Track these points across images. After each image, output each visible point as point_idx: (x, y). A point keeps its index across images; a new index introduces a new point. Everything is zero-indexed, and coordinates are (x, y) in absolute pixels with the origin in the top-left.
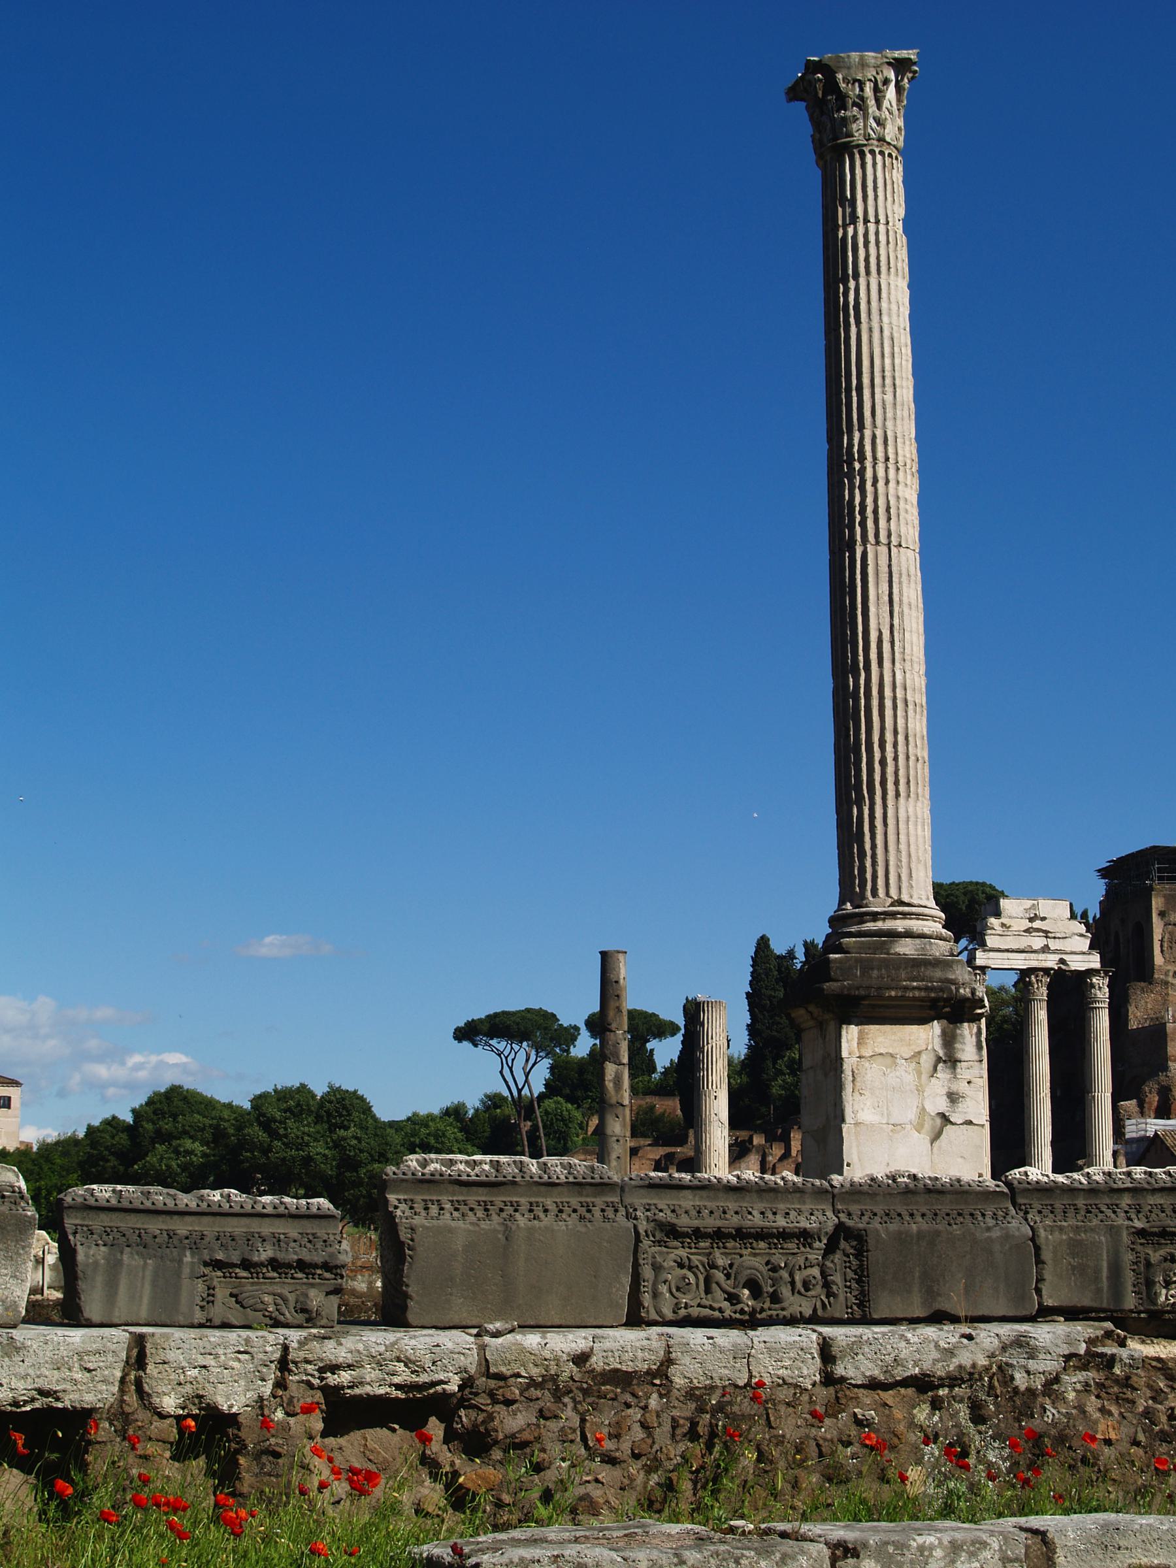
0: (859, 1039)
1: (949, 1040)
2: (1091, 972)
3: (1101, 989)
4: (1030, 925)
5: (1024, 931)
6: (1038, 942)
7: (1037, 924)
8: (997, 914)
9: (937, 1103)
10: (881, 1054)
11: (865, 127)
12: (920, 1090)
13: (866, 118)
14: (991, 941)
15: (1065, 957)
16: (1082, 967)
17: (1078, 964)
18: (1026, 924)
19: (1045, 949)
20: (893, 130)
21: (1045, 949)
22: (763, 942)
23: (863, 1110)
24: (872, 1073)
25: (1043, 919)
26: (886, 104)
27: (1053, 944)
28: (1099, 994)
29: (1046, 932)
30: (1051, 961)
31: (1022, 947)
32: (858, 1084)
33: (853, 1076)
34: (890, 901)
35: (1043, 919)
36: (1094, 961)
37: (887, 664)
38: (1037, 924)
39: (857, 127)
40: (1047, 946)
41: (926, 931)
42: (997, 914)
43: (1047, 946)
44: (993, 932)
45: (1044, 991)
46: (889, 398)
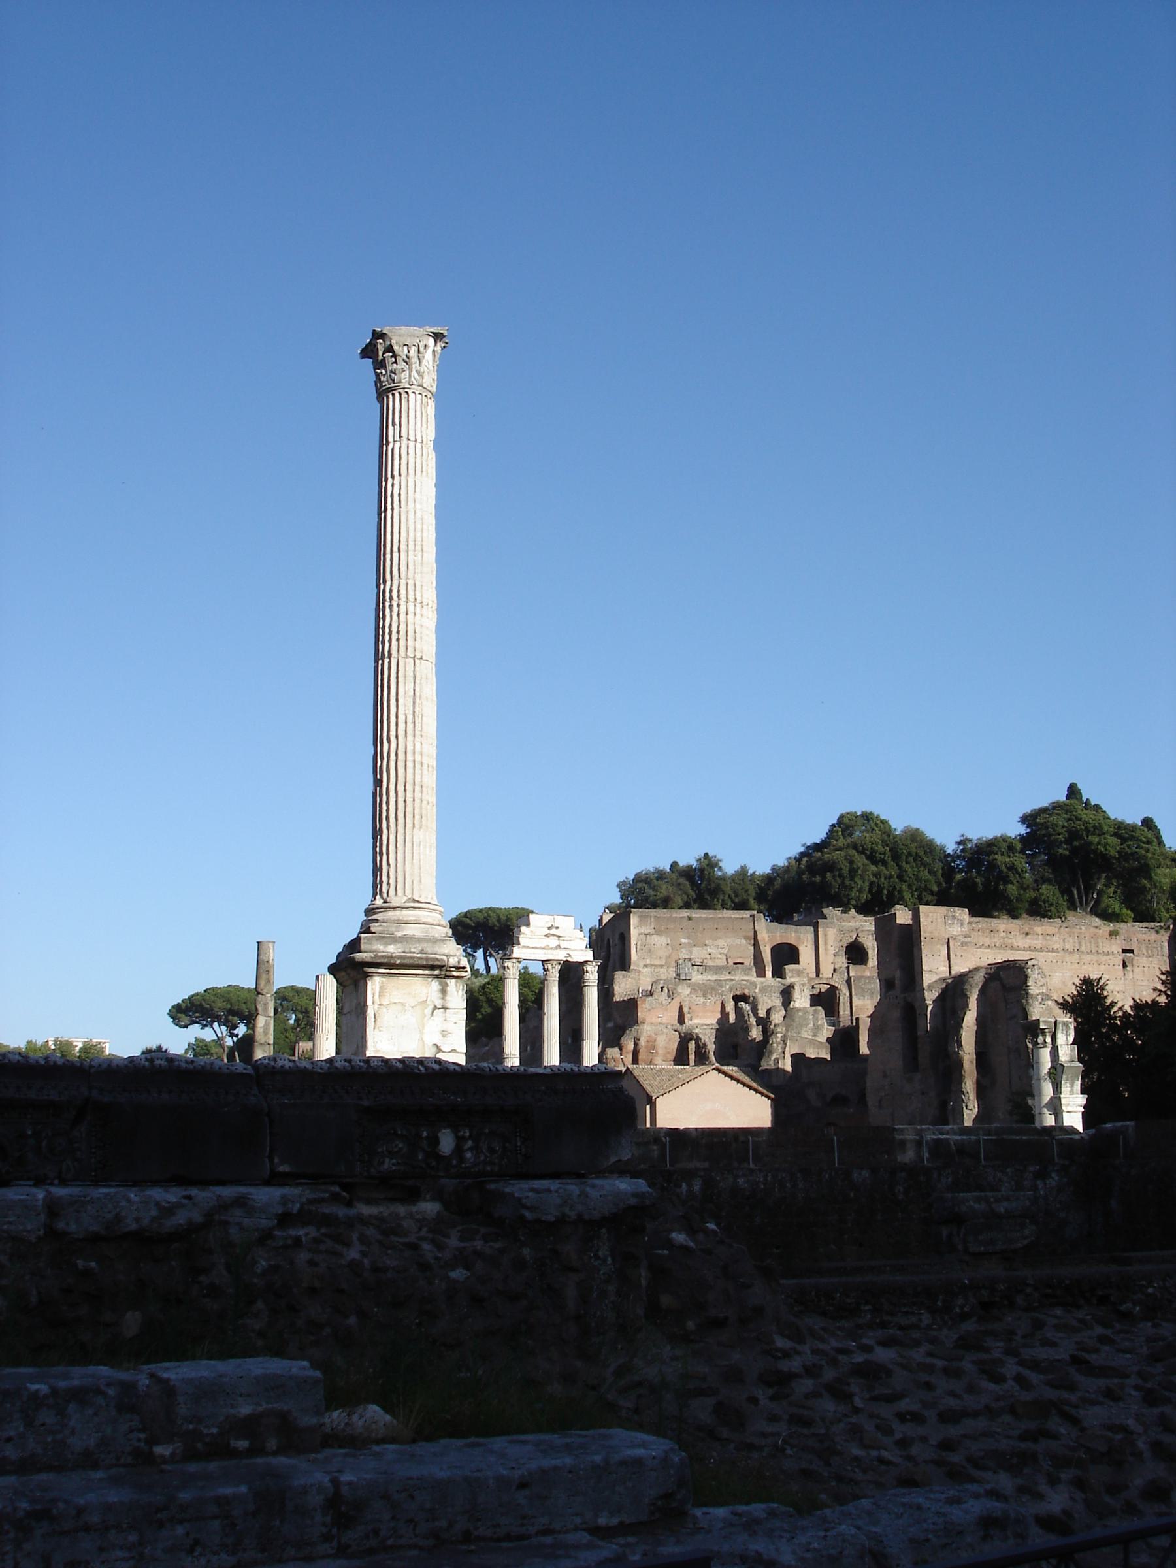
0: (380, 993)
1: (443, 991)
2: (586, 962)
3: (592, 976)
4: (548, 932)
5: (545, 936)
6: (553, 942)
7: (553, 931)
8: (528, 924)
10: (395, 1003)
11: (410, 376)
12: (422, 1027)
13: (411, 370)
15: (570, 953)
16: (582, 960)
17: (577, 957)
20: (430, 380)
23: (381, 1041)
24: (387, 1016)
25: (557, 928)
26: (424, 362)
28: (592, 977)
29: (559, 937)
30: (562, 956)
31: (543, 946)
32: (378, 1024)
33: (375, 1017)
34: (406, 898)
35: (557, 928)
36: (588, 955)
37: (410, 738)
38: (553, 931)
40: (559, 945)
41: (430, 920)
42: (528, 924)
43: (559, 945)
44: (524, 936)
46: (419, 558)
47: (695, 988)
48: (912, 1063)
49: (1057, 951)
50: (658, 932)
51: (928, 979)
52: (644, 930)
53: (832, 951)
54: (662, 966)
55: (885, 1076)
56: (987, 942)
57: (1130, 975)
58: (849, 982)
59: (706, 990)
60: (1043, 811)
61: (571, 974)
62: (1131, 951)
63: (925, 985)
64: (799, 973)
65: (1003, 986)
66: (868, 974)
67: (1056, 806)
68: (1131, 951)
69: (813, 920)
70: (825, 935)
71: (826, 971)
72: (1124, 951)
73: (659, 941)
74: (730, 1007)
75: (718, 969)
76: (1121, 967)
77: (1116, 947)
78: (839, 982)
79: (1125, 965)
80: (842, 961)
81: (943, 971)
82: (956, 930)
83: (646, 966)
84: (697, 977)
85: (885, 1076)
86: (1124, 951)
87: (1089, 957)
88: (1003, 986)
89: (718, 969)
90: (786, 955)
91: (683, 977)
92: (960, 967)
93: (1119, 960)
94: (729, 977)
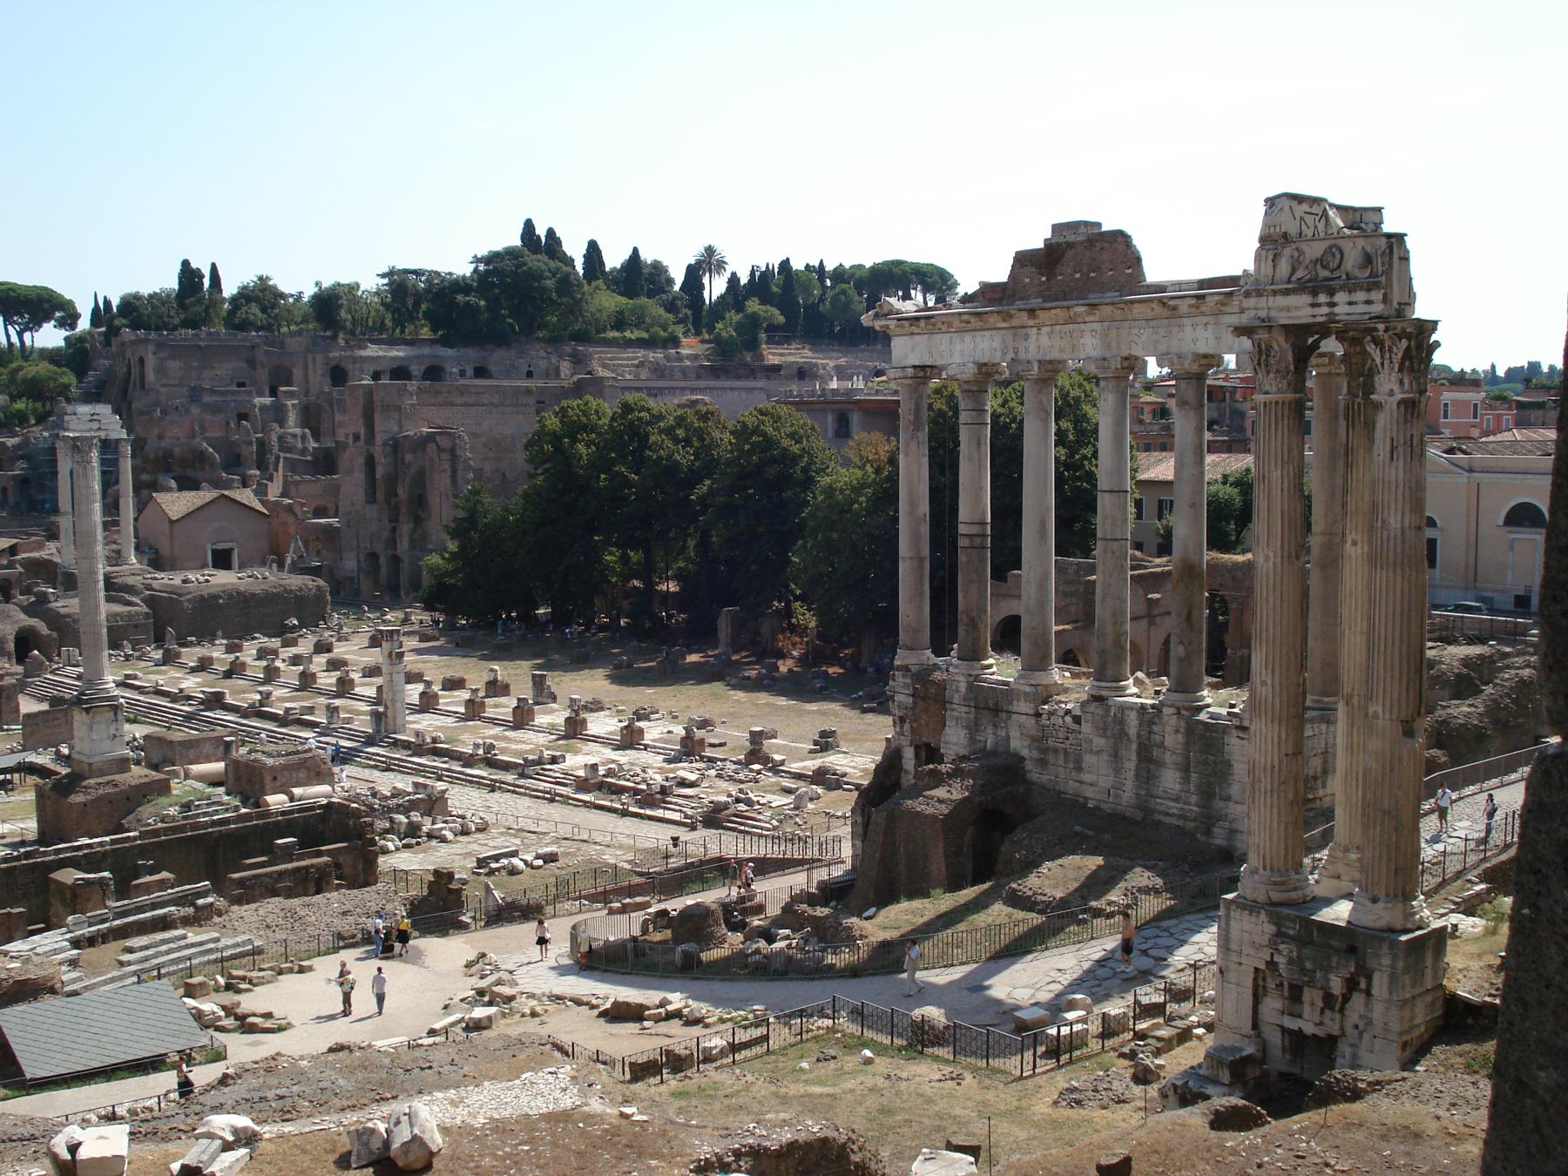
3: (128, 450)
6: (95, 425)
9: (112, 731)
17: (114, 436)
19: (99, 429)
21: (99, 429)
30: (103, 434)
48: (371, 498)
59: (215, 409)
61: (108, 446)
62: (543, 402)
64: (291, 395)
65: (438, 447)
67: (510, 253)
68: (543, 402)
70: (314, 359)
72: (538, 402)
83: (163, 385)
84: (207, 399)
86: (538, 402)
88: (438, 447)
93: (533, 410)
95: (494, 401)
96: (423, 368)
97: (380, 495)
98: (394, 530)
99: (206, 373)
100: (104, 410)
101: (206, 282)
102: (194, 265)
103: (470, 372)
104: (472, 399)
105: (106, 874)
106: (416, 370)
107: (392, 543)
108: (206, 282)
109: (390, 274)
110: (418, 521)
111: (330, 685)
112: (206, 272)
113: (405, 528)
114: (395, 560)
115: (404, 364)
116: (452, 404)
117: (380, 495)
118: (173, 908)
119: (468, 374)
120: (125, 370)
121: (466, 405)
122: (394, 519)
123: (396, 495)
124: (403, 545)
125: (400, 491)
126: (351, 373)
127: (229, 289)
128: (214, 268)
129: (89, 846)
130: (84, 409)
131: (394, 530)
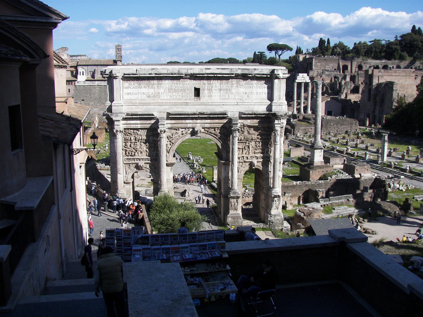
1: (321, 150)
2: (309, 82)
6: (303, 79)
7: (303, 77)
8: (298, 75)
9: (320, 155)
14: (298, 79)
16: (308, 82)
17: (307, 81)
18: (302, 77)
22: (255, 52)
24: (316, 153)
27: (305, 79)
30: (304, 81)
36: (310, 81)
38: (303, 77)
39: (319, 87)
42: (298, 75)
45: (304, 85)
47: (326, 75)
48: (369, 100)
49: (401, 76)
50: (318, 62)
51: (374, 84)
52: (316, 62)
53: (355, 67)
54: (319, 69)
55: (364, 101)
56: (387, 74)
57: (416, 80)
58: (358, 75)
59: (328, 75)
60: (405, 35)
61: (306, 84)
62: (417, 76)
63: (373, 85)
64: (348, 72)
66: (362, 72)
68: (417, 76)
69: (352, 60)
71: (353, 71)
72: (416, 75)
73: (319, 64)
74: (333, 79)
75: (331, 71)
76: (414, 79)
77: (414, 75)
78: (356, 74)
79: (415, 79)
80: (357, 69)
81: (377, 82)
82: (380, 74)
83: (316, 69)
84: (327, 73)
85: (364, 101)
86: (416, 75)
87: (408, 77)
89: (331, 71)
90: (345, 68)
91: (324, 73)
92: (381, 81)
93: (414, 77)
94: (333, 73)
95: (404, 75)
96: (382, 66)
97: (372, 99)
98: (375, 108)
99: (327, 66)
100: (305, 75)
101: (326, 43)
102: (323, 39)
103: (395, 67)
104: (397, 74)
105: (324, 189)
106: (380, 66)
107: (374, 112)
108: (326, 43)
109: (375, 41)
110: (381, 106)
111: (364, 147)
112: (326, 41)
113: (378, 108)
114: (374, 116)
115: (377, 64)
116: (392, 76)
117: (372, 99)
118: (343, 200)
119: (394, 68)
120: (306, 65)
121: (396, 76)
122: (375, 105)
123: (376, 99)
124: (377, 112)
125: (377, 98)
126: (363, 67)
127: (332, 45)
128: (328, 39)
129: (319, 182)
130: (301, 75)
131: (375, 108)
